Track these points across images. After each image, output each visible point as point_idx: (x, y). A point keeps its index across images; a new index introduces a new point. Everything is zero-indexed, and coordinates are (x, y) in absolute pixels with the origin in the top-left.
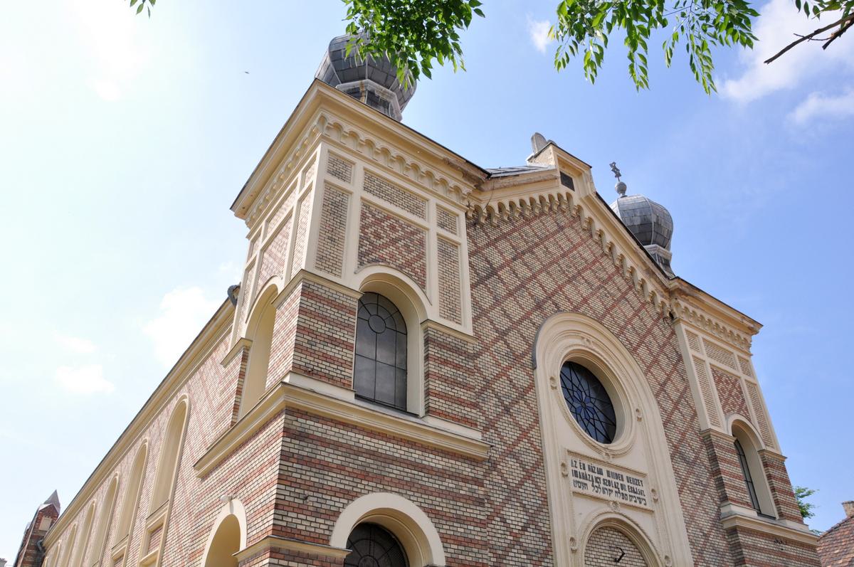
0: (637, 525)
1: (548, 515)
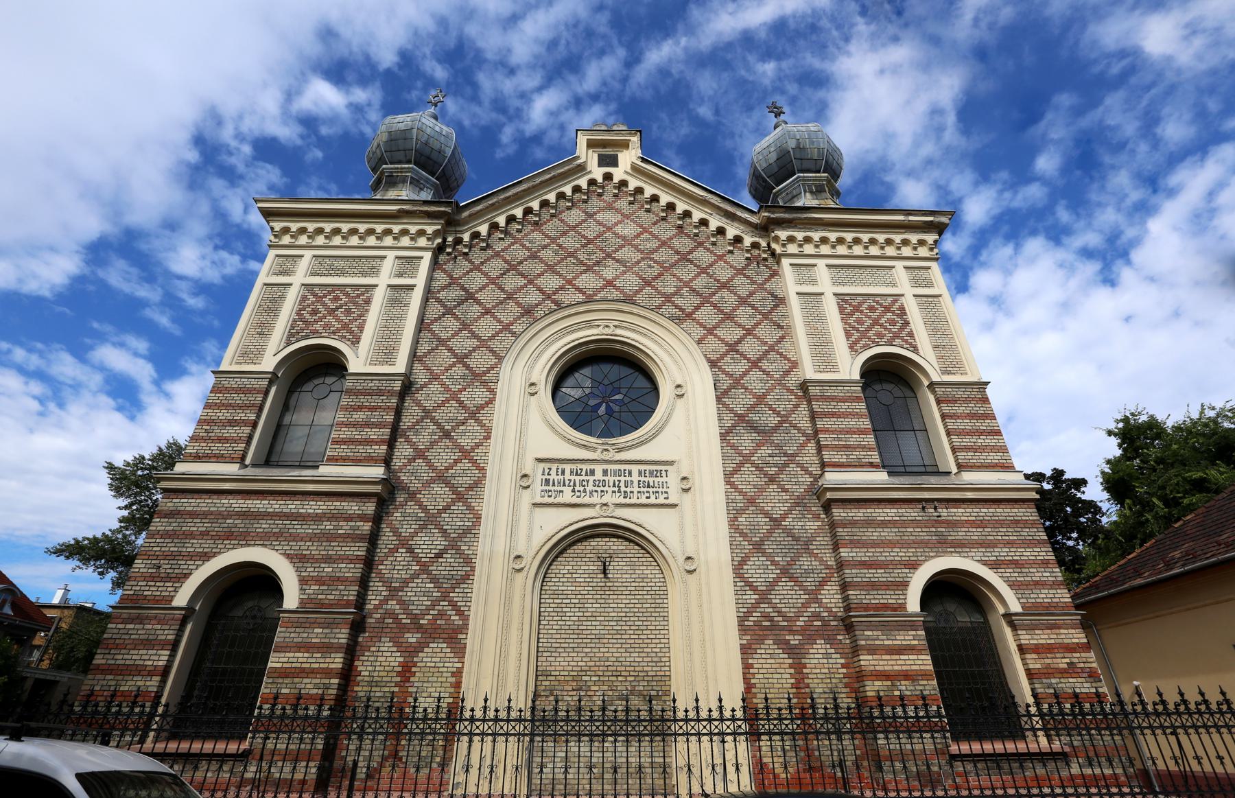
0: (640, 526)
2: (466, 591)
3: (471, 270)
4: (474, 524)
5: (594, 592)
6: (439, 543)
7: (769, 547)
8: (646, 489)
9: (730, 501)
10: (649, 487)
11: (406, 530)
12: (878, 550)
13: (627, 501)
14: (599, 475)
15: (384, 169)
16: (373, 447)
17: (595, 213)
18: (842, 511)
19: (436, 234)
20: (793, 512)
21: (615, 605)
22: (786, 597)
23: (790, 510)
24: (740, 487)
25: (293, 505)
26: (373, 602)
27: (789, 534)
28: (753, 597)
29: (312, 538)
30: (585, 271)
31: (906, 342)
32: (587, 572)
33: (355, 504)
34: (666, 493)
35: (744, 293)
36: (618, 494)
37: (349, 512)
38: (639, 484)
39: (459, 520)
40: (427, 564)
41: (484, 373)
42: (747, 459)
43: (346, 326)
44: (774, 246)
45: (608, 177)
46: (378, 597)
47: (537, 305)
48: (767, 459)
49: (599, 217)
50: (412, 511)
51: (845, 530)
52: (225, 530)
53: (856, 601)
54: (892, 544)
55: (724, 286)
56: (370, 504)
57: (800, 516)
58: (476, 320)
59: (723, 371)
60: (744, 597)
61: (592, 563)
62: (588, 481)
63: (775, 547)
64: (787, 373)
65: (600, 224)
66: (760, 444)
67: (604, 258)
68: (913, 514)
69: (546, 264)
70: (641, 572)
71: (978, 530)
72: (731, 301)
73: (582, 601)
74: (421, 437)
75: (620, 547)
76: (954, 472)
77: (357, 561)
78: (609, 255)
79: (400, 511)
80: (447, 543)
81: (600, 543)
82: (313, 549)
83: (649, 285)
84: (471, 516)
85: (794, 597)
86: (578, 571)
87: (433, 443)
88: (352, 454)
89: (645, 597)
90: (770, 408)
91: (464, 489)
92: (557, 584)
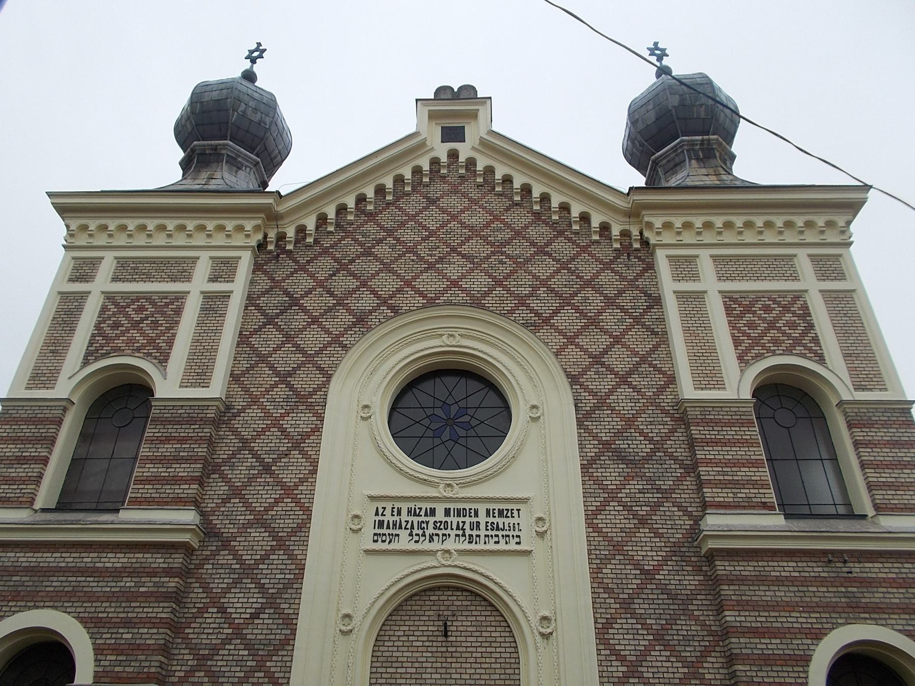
1: (298, 591)
2: (285, 659)
3: (296, 271)
4: (297, 576)
5: (434, 660)
6: (255, 600)
7: (640, 607)
8: (494, 533)
9: (593, 547)
10: (498, 529)
11: (217, 585)
12: (773, 614)
13: (473, 547)
14: (440, 516)
15: (195, 146)
16: (182, 487)
17: (438, 199)
18: (727, 563)
19: (257, 228)
20: (669, 563)
21: (458, 676)
22: (660, 670)
23: (665, 560)
24: (604, 530)
25: (88, 559)
26: (177, 674)
27: (664, 589)
28: (620, 669)
29: (110, 597)
30: (426, 270)
31: (810, 350)
32: (425, 633)
33: (160, 556)
34: (518, 536)
35: (611, 292)
36: (462, 539)
37: (153, 565)
38: (487, 526)
39: (279, 571)
40: (241, 627)
41: (311, 395)
42: (612, 496)
43: (151, 341)
44: (646, 234)
45: (453, 155)
46: (184, 668)
47: (371, 312)
48: (637, 495)
49: (443, 203)
50: (225, 562)
51: (732, 587)
52: (11, 589)
53: (744, 679)
54: (790, 607)
55: (588, 284)
56: (177, 556)
57: (677, 568)
58: (301, 331)
59: (586, 389)
60: (610, 669)
61: (432, 623)
62: (427, 523)
63: (647, 606)
64: (661, 390)
65: (443, 211)
66: (627, 478)
67: (448, 254)
68: (817, 569)
69: (382, 263)
70: (488, 634)
71: (901, 590)
72: (597, 302)
73: (419, 670)
74: (238, 472)
75: (464, 603)
76: (870, 515)
77: (161, 625)
78: (453, 250)
79: (211, 562)
80: (264, 601)
81: (442, 598)
82: (110, 611)
83: (500, 285)
84: (293, 567)
85: (670, 670)
86: (416, 633)
87: (251, 479)
88: (158, 495)
89: (493, 666)
90: (641, 433)
91: (285, 534)
92: (390, 649)
